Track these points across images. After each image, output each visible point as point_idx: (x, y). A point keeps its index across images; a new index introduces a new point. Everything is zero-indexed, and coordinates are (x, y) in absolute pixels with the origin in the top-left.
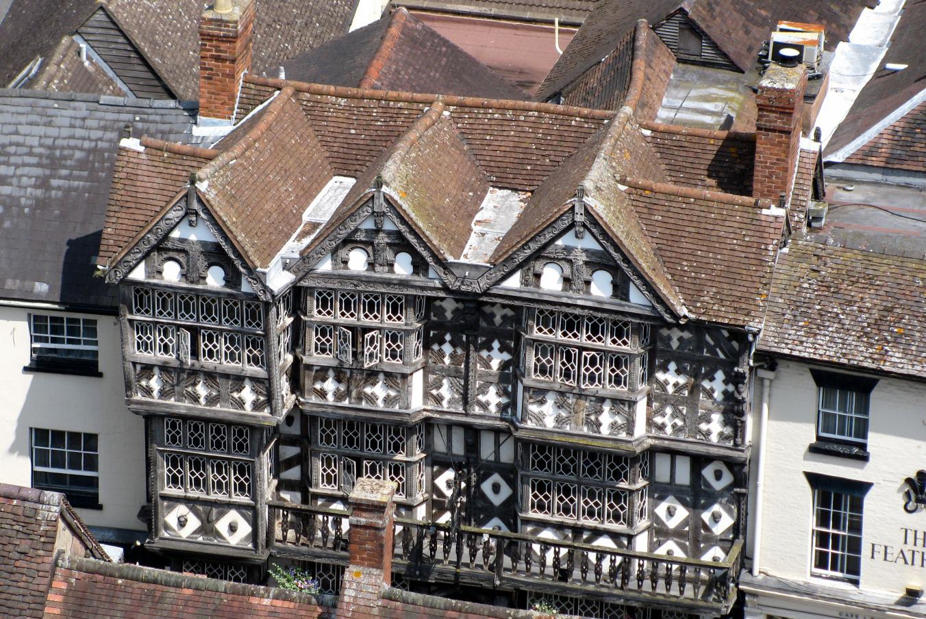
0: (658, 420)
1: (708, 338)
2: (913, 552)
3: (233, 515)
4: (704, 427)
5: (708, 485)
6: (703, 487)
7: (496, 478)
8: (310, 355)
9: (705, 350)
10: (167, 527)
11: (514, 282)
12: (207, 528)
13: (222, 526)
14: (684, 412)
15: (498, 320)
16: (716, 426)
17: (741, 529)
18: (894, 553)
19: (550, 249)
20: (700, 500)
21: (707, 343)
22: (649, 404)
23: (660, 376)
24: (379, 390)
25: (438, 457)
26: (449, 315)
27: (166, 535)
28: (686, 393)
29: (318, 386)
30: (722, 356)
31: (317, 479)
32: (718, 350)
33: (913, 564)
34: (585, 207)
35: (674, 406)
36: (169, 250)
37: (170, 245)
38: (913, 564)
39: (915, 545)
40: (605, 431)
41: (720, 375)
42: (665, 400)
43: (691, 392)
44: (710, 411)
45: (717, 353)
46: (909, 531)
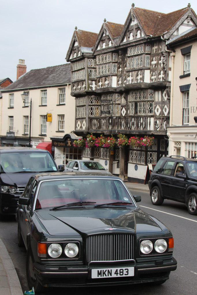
0: (152, 78)
3: (84, 122)
10: (77, 127)
11: (125, 41)
12: (81, 127)
17: (169, 113)
19: (130, 27)
22: (150, 73)
24: (107, 82)
27: (77, 129)
29: (99, 84)
37: (74, 49)
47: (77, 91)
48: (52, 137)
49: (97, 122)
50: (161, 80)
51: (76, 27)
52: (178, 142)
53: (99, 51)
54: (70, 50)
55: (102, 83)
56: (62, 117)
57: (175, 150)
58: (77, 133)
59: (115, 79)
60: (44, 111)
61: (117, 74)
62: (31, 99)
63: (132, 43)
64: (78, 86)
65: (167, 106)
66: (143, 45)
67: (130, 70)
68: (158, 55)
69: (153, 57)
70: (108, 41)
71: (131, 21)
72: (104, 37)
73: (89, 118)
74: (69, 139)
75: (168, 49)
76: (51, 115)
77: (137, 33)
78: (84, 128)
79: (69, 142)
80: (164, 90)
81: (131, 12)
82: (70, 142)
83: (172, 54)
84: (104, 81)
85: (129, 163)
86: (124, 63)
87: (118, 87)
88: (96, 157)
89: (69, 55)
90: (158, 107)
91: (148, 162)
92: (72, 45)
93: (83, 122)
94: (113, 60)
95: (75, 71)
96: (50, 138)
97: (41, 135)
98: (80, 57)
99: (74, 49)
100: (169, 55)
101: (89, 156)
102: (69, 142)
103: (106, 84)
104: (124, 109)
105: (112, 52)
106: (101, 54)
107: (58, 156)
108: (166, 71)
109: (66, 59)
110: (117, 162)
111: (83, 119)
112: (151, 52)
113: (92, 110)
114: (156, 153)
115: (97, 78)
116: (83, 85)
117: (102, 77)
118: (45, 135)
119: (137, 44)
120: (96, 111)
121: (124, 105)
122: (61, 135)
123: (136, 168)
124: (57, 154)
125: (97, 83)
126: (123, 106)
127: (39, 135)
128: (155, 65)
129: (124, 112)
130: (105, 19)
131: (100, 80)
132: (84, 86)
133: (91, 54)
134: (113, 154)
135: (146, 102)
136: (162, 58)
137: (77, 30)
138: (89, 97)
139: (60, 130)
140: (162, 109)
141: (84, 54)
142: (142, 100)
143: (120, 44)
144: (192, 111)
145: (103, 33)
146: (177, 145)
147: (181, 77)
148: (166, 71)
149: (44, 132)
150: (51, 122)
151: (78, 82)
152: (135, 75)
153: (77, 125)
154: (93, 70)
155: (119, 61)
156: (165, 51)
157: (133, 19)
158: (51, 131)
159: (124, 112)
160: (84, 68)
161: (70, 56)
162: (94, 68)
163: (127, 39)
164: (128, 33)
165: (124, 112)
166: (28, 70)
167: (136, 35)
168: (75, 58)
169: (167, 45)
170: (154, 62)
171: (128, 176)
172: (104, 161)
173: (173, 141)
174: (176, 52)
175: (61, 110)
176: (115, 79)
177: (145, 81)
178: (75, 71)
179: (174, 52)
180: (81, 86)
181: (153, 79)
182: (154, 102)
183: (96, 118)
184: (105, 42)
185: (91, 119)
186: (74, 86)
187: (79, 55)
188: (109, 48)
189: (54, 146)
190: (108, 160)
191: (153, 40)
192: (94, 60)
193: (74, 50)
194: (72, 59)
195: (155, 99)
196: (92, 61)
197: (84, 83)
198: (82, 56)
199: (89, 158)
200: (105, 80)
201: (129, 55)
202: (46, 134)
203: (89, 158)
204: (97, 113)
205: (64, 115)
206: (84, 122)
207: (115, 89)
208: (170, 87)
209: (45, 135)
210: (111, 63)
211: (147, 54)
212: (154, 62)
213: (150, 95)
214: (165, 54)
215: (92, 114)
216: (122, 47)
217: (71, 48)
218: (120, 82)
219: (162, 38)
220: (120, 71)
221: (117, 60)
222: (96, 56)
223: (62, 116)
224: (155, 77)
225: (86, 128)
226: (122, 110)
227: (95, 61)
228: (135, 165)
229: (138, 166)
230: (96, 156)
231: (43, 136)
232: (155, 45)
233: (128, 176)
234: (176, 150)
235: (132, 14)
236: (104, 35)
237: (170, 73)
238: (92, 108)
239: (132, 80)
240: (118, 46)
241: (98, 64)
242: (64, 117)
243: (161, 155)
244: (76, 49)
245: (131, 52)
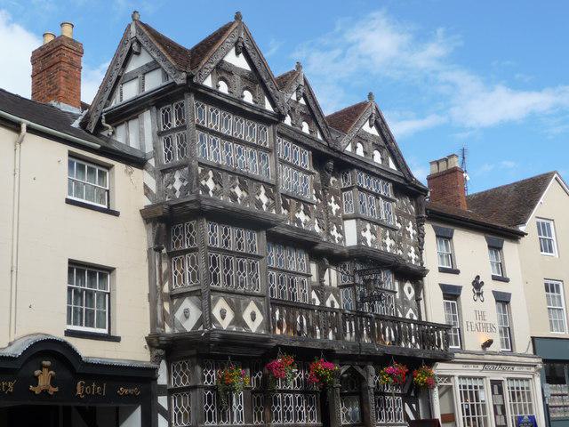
3: (252, 307)
12: (238, 320)
13: (246, 317)
16: (412, 255)
40: (388, 250)
65: (415, 312)
79: (44, 379)
93: (246, 305)
102: (44, 379)
147: (442, 270)
206: (252, 307)
244: (230, 73)
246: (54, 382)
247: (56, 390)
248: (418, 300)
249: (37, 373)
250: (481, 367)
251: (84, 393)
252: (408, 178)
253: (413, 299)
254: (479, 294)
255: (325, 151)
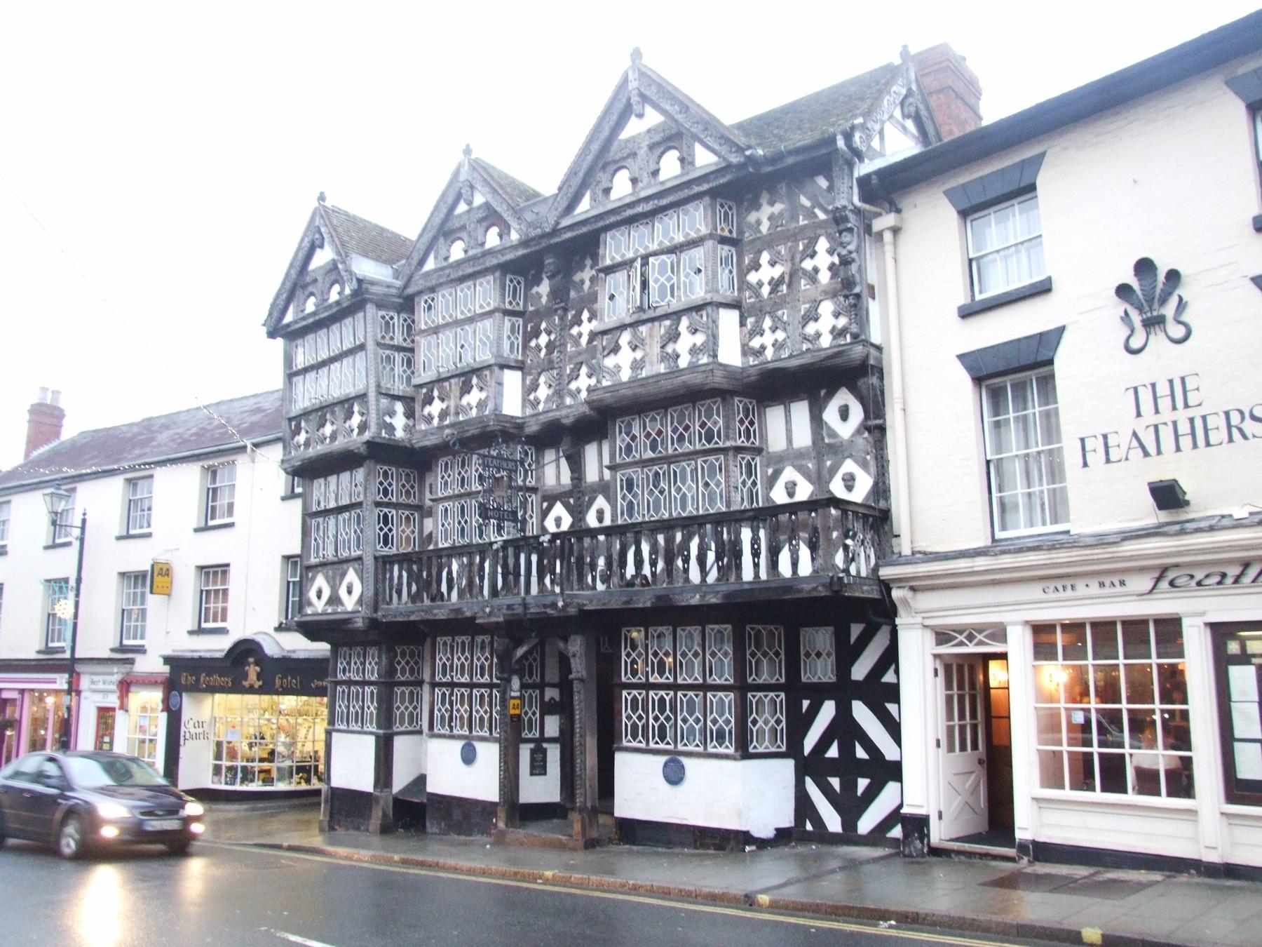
0: (756, 343)
1: (805, 201)
2: (1156, 427)
3: (351, 576)
4: (811, 329)
5: (833, 434)
6: (827, 441)
7: (601, 502)
8: (420, 375)
9: (801, 217)
10: (310, 604)
12: (334, 600)
13: (343, 592)
14: (785, 318)
15: (587, 284)
17: (881, 489)
18: (1120, 441)
20: (824, 462)
21: (802, 206)
22: (742, 324)
23: (753, 278)
24: (474, 397)
25: (546, 490)
26: (544, 300)
28: (784, 288)
29: (427, 410)
30: (822, 216)
31: (437, 537)
32: (817, 211)
33: (1159, 452)
34: (639, 70)
35: (772, 314)
36: (308, 284)
37: (308, 279)
38: (1159, 452)
39: (1157, 411)
41: (823, 244)
42: (760, 310)
43: (789, 286)
44: (816, 304)
45: (814, 213)
46: (1140, 390)
47: (318, 449)
48: (169, 652)
49: (405, 574)
50: (826, 341)
51: (322, 193)
52: (961, 632)
53: (428, 274)
54: (289, 285)
55: (444, 406)
56: (215, 573)
57: (936, 671)
58: (312, 630)
59: (512, 380)
60: (139, 557)
61: (523, 362)
62: (84, 514)
63: (631, 205)
64: (323, 425)
65: (864, 465)
66: (707, 200)
67: (628, 320)
68: (794, 236)
69: (760, 252)
70: (481, 230)
71: (626, 113)
72: (460, 216)
73: (376, 558)
74: (251, 660)
75: (865, 198)
76: (168, 570)
77: (658, 163)
78: (349, 603)
79: (253, 671)
80: (831, 394)
81: (631, 77)
82: (258, 669)
83: (878, 225)
84: (456, 391)
85: (627, 749)
86: (565, 310)
87: (529, 411)
88: (402, 729)
89: (279, 309)
90: (789, 474)
91: (752, 741)
92: (298, 264)
93: (343, 575)
94: (504, 303)
95: (305, 370)
96: (162, 660)
97: (122, 649)
98: (338, 303)
99: (308, 279)
100: (868, 230)
101: (373, 729)
102: (253, 671)
103: (469, 404)
104: (559, 509)
105: (506, 268)
106: (441, 285)
107: (193, 731)
108: (858, 296)
109: (264, 325)
110: (532, 746)
111: (345, 566)
112: (740, 232)
113: (386, 523)
114: (783, 695)
115: (421, 386)
116: (349, 415)
117: (447, 379)
118: (140, 650)
119: (664, 202)
120: (403, 531)
121: (555, 492)
122: (218, 646)
123: (674, 775)
124: (191, 723)
125: (417, 407)
126: (551, 499)
127: (113, 650)
128: (775, 284)
129: (558, 521)
130: (468, 146)
131: (436, 393)
132: (356, 420)
133: (394, 291)
134: (517, 712)
135: (731, 453)
136: (823, 244)
137: (328, 204)
138: (375, 469)
139: (204, 625)
140: (820, 479)
141: (364, 286)
142: (698, 447)
143: (557, 223)
144: (1096, 459)
145: (459, 197)
146: (961, 644)
147: (968, 312)
148: (858, 296)
149: (135, 638)
150: (169, 595)
151: (321, 412)
152: (657, 339)
153: (312, 594)
154: (398, 357)
155: (531, 309)
156: (851, 207)
157: (637, 108)
158: (168, 633)
159: (558, 521)
160: (362, 347)
161: (284, 312)
162: (399, 349)
163: (593, 199)
164: (602, 177)
165: (559, 518)
166: (69, 432)
167: (655, 173)
168: (314, 314)
169: (864, 182)
170: (766, 273)
171: (617, 814)
172: (458, 745)
173: (926, 627)
174: (908, 214)
175: (213, 549)
176: (512, 380)
177: (723, 358)
178: (305, 370)
179: (898, 211)
180: (335, 427)
181: (763, 348)
182: (764, 452)
183: (403, 559)
184: (464, 235)
185: (384, 562)
186: (297, 431)
187: (334, 296)
188: (491, 252)
189: (182, 689)
190: (483, 739)
191: (768, 169)
192: (404, 315)
193: (304, 287)
194: (295, 322)
195: (763, 437)
196: (392, 318)
197: (356, 408)
198: (355, 293)
199: (371, 733)
200: (466, 389)
201: (608, 262)
202: (143, 646)
203: (371, 733)
204: (408, 538)
205: (228, 565)
206: (351, 576)
207: (520, 426)
208: (881, 371)
209: (140, 650)
210: (498, 315)
211: (723, 241)
212: (766, 273)
213: (742, 422)
214: (853, 221)
215: (386, 543)
216: (569, 235)
217: (294, 276)
218: (543, 392)
219: (841, 143)
220: (538, 348)
221: (521, 303)
222: (417, 299)
223: (215, 573)
224: (780, 335)
225: (360, 601)
226: (545, 514)
227: (405, 320)
228: (662, 759)
229: (685, 761)
230: (402, 724)
231: (125, 654)
232: (764, 200)
233: (617, 814)
234: (941, 673)
235: (633, 85)
236: (462, 208)
237: (874, 307)
238: (386, 516)
239: (637, 365)
240: (542, 237)
241: (423, 327)
242: (225, 573)
243: (806, 703)
244: (315, 281)
245: (615, 248)
246: (259, 676)
247: (260, 683)
248: (875, 429)
249: (247, 668)
250: (1145, 583)
251: (282, 686)
252: (735, 159)
253: (858, 432)
254: (1153, 323)
255: (521, 252)
